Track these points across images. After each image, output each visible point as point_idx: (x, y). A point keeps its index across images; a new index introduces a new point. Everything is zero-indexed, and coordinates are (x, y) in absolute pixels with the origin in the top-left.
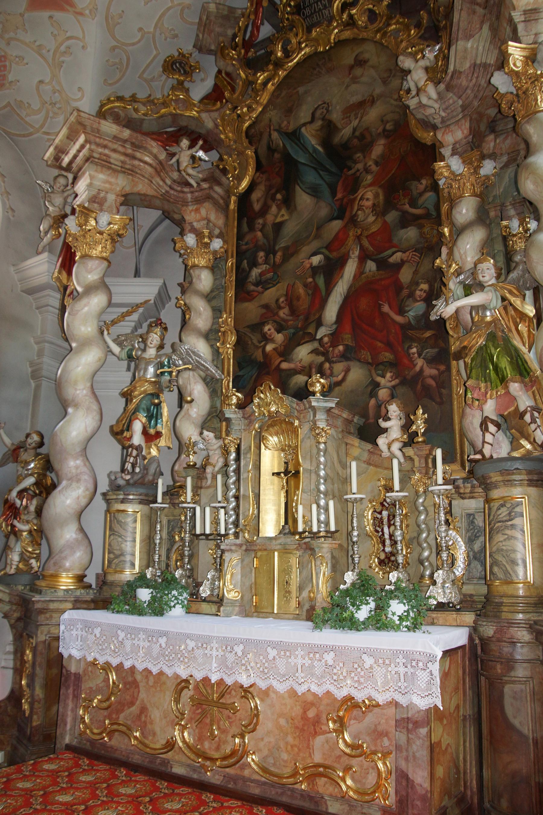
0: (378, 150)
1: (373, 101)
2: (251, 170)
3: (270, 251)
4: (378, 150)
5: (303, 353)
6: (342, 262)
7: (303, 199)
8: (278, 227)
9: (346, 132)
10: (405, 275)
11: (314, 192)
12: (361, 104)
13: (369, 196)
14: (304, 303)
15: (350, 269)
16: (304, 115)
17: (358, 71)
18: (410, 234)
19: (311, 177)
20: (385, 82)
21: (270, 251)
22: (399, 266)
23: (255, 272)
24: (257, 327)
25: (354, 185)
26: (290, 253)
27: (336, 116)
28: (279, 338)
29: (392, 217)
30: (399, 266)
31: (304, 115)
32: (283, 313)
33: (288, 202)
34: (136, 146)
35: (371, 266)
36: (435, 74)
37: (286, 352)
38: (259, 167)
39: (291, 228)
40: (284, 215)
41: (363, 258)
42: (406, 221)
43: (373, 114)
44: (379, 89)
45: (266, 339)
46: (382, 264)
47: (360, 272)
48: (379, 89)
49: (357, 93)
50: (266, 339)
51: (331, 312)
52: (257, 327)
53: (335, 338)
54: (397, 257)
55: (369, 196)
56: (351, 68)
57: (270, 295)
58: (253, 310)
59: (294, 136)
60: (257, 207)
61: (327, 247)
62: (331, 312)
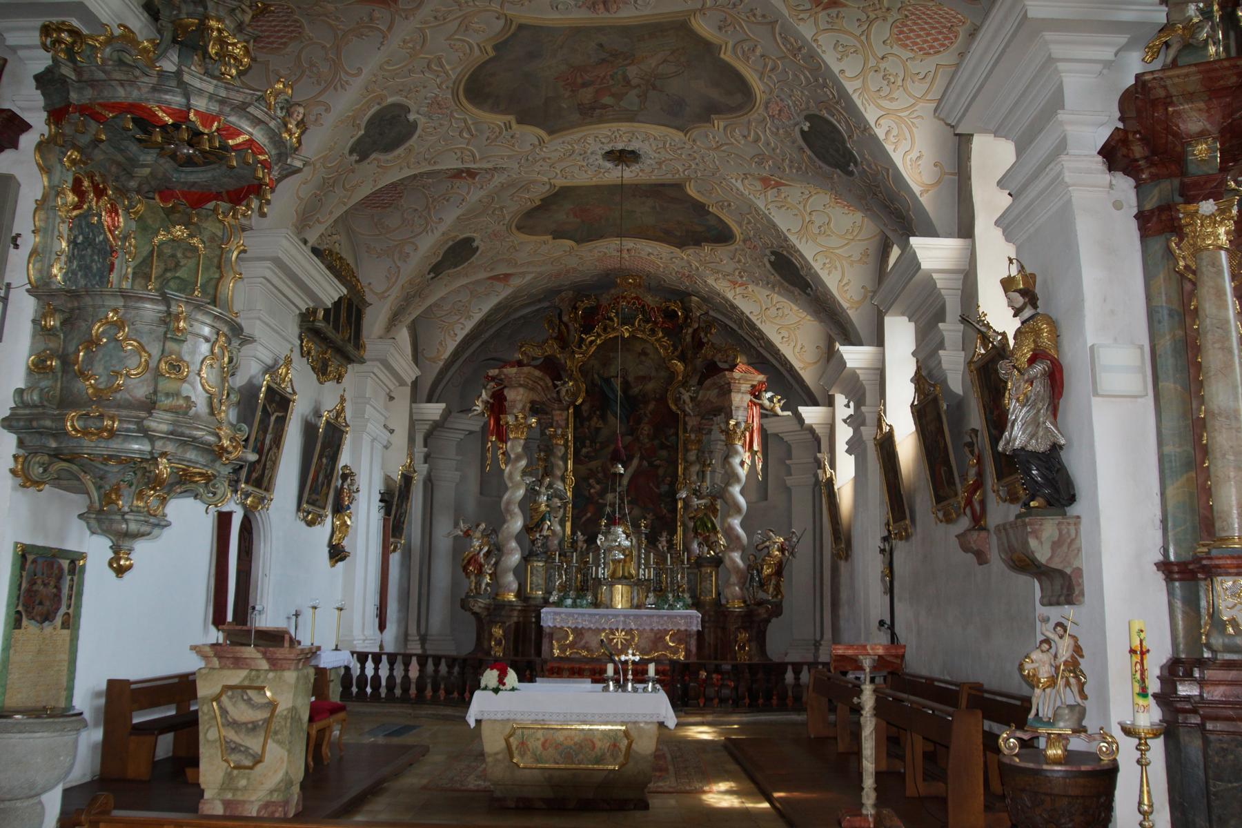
0: (651, 406)
1: (650, 379)
2: (583, 394)
4: (651, 406)
8: (598, 430)
9: (636, 390)
10: (661, 472)
12: (644, 378)
13: (646, 429)
17: (643, 358)
18: (664, 453)
20: (657, 370)
22: (658, 467)
23: (584, 450)
27: (630, 379)
28: (598, 487)
29: (656, 442)
30: (658, 467)
32: (600, 475)
33: (603, 417)
34: (541, 379)
35: (645, 463)
36: (692, 399)
37: (602, 494)
38: (587, 392)
40: (600, 424)
41: (642, 459)
42: (663, 446)
43: (650, 386)
44: (653, 374)
45: (592, 487)
46: (650, 464)
47: (640, 465)
48: (653, 374)
50: (592, 487)
54: (658, 462)
55: (646, 429)
56: (640, 354)
57: (594, 464)
59: (607, 381)
60: (585, 414)
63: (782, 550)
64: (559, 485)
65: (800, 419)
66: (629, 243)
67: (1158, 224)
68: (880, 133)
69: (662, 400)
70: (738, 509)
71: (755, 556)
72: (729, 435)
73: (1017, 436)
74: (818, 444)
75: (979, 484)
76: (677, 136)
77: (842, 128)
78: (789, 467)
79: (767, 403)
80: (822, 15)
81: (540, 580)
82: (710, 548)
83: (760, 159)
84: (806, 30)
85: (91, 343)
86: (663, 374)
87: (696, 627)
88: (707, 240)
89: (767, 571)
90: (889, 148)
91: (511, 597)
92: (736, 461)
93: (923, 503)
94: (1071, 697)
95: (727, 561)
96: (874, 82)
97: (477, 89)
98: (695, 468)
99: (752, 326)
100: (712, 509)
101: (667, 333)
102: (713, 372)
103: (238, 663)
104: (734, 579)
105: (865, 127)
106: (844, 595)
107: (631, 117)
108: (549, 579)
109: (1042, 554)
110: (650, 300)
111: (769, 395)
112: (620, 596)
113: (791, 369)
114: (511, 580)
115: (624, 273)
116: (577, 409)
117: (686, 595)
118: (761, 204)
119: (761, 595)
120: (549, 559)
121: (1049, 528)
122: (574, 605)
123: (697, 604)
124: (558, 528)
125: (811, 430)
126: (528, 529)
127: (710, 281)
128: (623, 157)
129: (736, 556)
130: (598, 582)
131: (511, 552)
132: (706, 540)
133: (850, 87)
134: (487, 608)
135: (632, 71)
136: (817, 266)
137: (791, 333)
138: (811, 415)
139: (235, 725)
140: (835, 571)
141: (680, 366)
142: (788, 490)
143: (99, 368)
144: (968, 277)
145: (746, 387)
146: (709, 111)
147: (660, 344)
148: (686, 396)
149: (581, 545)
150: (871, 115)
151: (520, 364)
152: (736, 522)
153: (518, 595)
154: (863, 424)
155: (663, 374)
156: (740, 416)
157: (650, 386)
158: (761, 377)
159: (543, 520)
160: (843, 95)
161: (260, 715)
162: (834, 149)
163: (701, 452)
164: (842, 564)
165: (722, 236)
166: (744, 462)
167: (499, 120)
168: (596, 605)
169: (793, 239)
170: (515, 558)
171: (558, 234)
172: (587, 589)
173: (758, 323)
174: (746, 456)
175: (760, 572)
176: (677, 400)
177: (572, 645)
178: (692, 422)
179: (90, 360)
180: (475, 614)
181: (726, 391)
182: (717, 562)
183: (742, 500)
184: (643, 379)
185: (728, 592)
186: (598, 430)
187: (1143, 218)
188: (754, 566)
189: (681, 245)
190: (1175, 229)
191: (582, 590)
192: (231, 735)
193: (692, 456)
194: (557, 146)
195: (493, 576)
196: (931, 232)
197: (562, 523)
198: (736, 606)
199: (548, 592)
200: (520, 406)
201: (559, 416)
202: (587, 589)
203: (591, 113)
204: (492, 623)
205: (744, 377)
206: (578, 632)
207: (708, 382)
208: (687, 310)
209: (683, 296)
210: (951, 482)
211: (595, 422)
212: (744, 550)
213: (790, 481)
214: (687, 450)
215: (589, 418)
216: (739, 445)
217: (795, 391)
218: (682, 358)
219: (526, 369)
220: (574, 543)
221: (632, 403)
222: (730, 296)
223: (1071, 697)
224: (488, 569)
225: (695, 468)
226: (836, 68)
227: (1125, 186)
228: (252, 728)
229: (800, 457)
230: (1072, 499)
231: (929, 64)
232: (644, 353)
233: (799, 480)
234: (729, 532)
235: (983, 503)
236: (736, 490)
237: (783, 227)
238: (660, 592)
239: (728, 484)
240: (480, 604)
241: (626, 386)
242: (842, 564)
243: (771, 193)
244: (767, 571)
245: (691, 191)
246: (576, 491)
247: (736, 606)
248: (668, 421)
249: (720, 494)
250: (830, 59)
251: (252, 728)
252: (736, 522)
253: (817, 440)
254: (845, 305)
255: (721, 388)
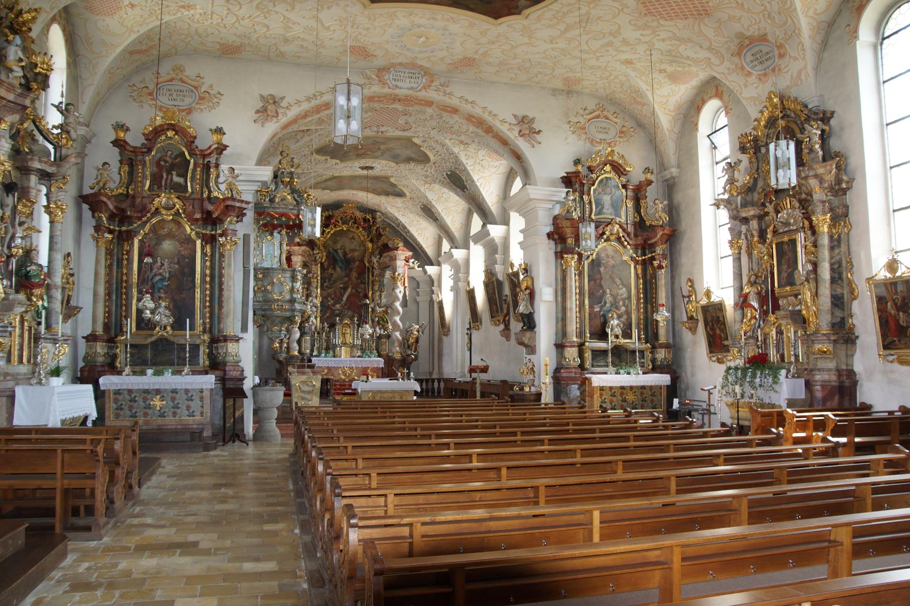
3: (330, 280)
4: (357, 263)
5: (338, 306)
6: (348, 288)
7: (338, 269)
8: (332, 274)
9: (349, 256)
11: (341, 268)
14: (338, 295)
15: (349, 290)
16: (339, 246)
18: (362, 286)
19: (340, 264)
21: (330, 280)
24: (326, 298)
25: (351, 270)
26: (335, 282)
27: (347, 250)
31: (339, 246)
33: (334, 269)
37: (334, 305)
39: (335, 276)
40: (333, 272)
41: (352, 288)
43: (356, 254)
49: (353, 246)
51: (345, 299)
52: (326, 298)
53: (345, 304)
55: (354, 274)
57: (330, 291)
58: (325, 293)
59: (336, 251)
61: (345, 283)
62: (345, 299)
63: (418, 331)
64: (315, 301)
65: (425, 272)
66: (355, 192)
67: (559, 255)
68: (478, 184)
69: (362, 261)
70: (399, 313)
71: (407, 333)
72: (394, 279)
73: (521, 309)
74: (432, 283)
75: (508, 314)
76: (393, 164)
77: (464, 178)
78: (418, 293)
79: (411, 264)
80: (462, 146)
81: (309, 346)
82: (385, 330)
83: (427, 177)
84: (456, 150)
85: (273, 284)
86: (362, 248)
87: (382, 365)
88: (392, 195)
89: (411, 341)
90: (481, 189)
91: (296, 353)
92: (397, 291)
93: (485, 316)
94: (532, 377)
95: (394, 337)
96: (478, 167)
97: (321, 151)
98: (378, 293)
99: (405, 228)
100: (386, 312)
101: (364, 228)
102: (386, 248)
103: (304, 373)
104: (396, 344)
105: (473, 181)
106: (445, 351)
107: (376, 158)
108: (313, 346)
109: (526, 342)
110: (358, 214)
111: (413, 260)
112: (344, 352)
113: (421, 247)
114: (295, 346)
115: (348, 202)
116: (322, 264)
117: (375, 351)
118: (422, 189)
119: (409, 352)
120: (313, 336)
121: (528, 334)
122: (326, 356)
123: (379, 356)
124: (315, 322)
125: (430, 276)
126: (302, 323)
127: (389, 209)
128: (367, 168)
129: (398, 334)
130: (335, 346)
131: (295, 333)
132: (383, 326)
133: (469, 168)
134: (286, 358)
135: (382, 147)
136: (443, 214)
137: (424, 234)
138: (431, 270)
139: (304, 392)
140: (440, 341)
141: (370, 245)
142: (418, 303)
143: (276, 290)
144: (506, 240)
145: (403, 257)
146: (409, 160)
147: (361, 233)
148: (375, 260)
149: (327, 329)
150: (475, 178)
151: (299, 244)
152: (397, 319)
153: (300, 352)
154: (459, 280)
155: (362, 248)
156: (400, 270)
157: (356, 254)
158: (411, 253)
159: (309, 317)
160: (466, 169)
161: (311, 389)
162: (458, 181)
163: (380, 285)
164: (445, 338)
165: (400, 195)
166: (400, 291)
167: (323, 158)
168: (334, 356)
169: (434, 203)
170: (298, 335)
171: (324, 189)
172: (330, 348)
173: (408, 227)
174: (402, 289)
175: (408, 341)
176: (370, 262)
177: (326, 374)
178: (376, 272)
179: (273, 289)
180: (280, 362)
181: (394, 259)
182: (388, 337)
183: (400, 309)
184: (353, 250)
185: (393, 350)
186: (332, 274)
187: (556, 253)
188: (405, 339)
189: (379, 194)
190: (562, 258)
191: (327, 349)
192: (303, 395)
193: (376, 288)
194: (343, 165)
195: (288, 344)
196: (495, 223)
197: (316, 318)
198: (398, 356)
199: (312, 351)
200: (299, 264)
201: (314, 268)
202: (330, 348)
203: (359, 156)
204: (288, 365)
205: (402, 254)
206: (329, 368)
207: (385, 254)
208: (374, 218)
209: (373, 212)
210: (497, 311)
211: (330, 271)
212: (401, 331)
213: (418, 299)
214: (373, 285)
215: (328, 269)
216: (399, 284)
217: (421, 257)
218: (371, 241)
219: (303, 248)
220: (323, 327)
221: (348, 262)
222: (396, 215)
223: (532, 377)
224: (286, 340)
225: (378, 293)
226: (465, 162)
227: (552, 243)
228: (309, 392)
229: (424, 288)
230: (535, 327)
231: (498, 163)
232: (353, 238)
233: (423, 299)
234: (395, 324)
235: (509, 320)
236: (398, 304)
237: (430, 198)
238: (363, 350)
239: (394, 301)
240: (283, 356)
241: (345, 254)
242: (445, 338)
243: (427, 186)
244: (411, 341)
245: (392, 180)
246: (322, 303)
247: (398, 356)
248: (364, 271)
249: (389, 307)
250: (463, 159)
251: (309, 392)
252: (397, 319)
253: (432, 281)
254: (453, 230)
255: (391, 257)
